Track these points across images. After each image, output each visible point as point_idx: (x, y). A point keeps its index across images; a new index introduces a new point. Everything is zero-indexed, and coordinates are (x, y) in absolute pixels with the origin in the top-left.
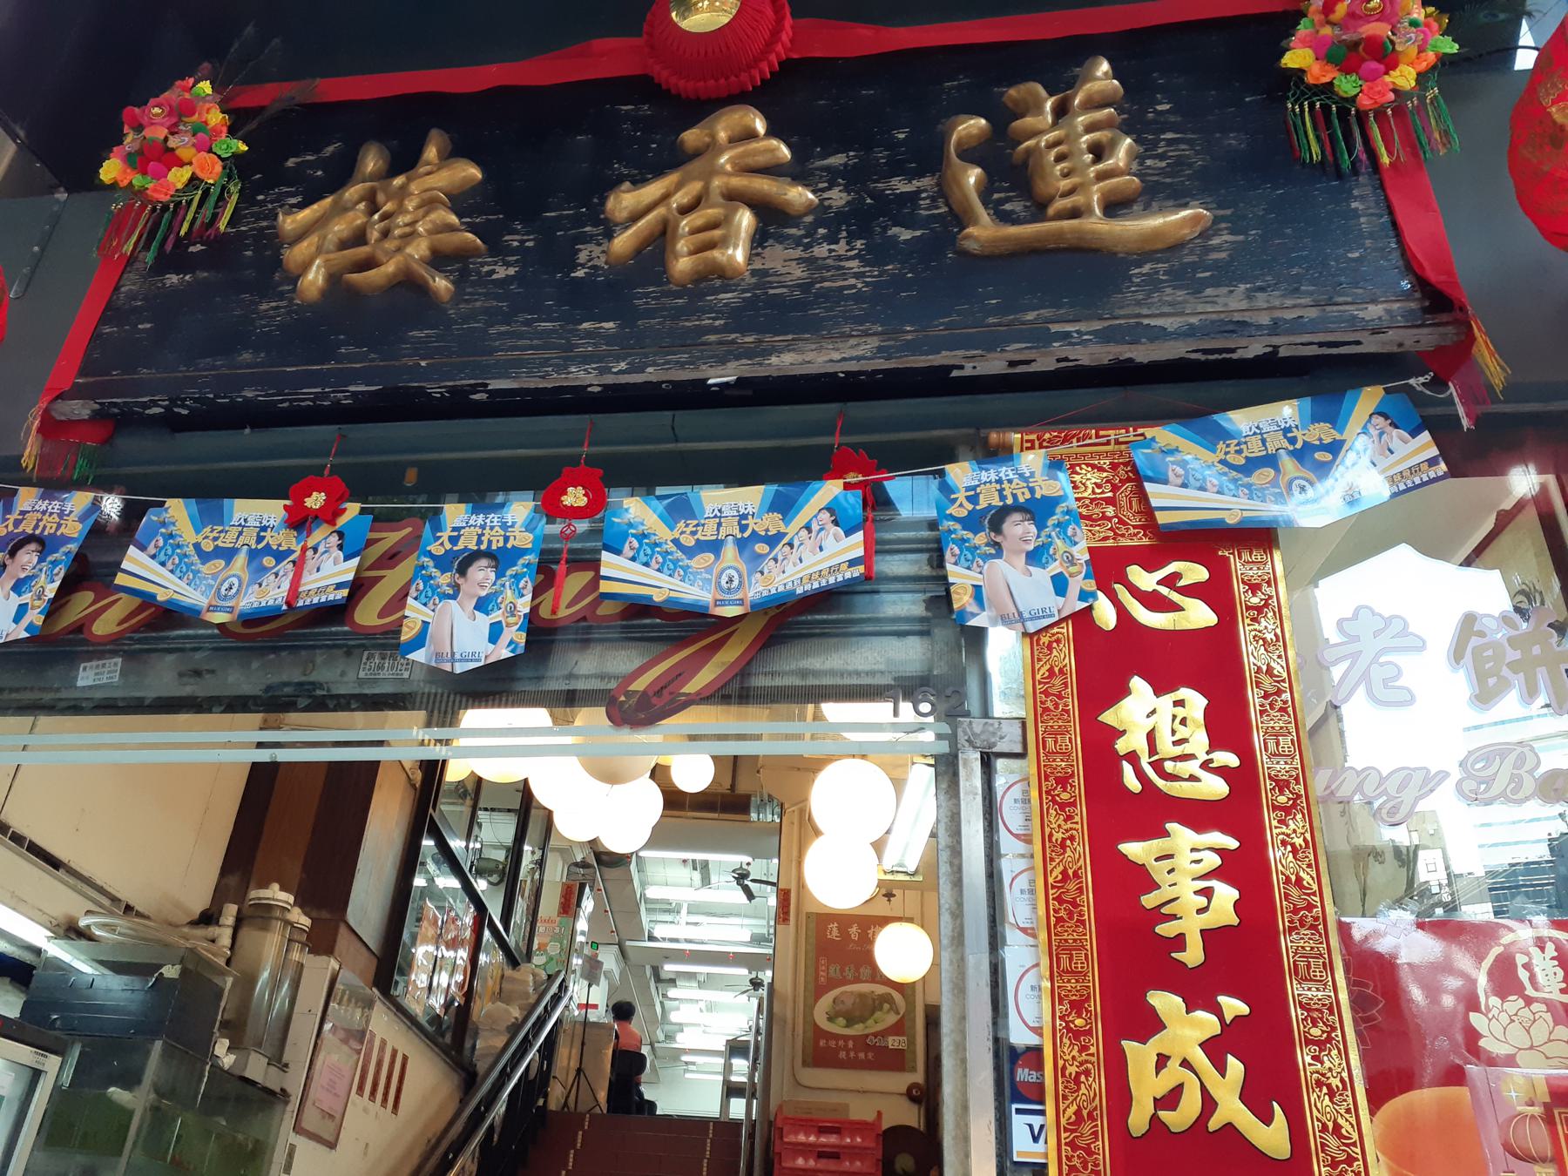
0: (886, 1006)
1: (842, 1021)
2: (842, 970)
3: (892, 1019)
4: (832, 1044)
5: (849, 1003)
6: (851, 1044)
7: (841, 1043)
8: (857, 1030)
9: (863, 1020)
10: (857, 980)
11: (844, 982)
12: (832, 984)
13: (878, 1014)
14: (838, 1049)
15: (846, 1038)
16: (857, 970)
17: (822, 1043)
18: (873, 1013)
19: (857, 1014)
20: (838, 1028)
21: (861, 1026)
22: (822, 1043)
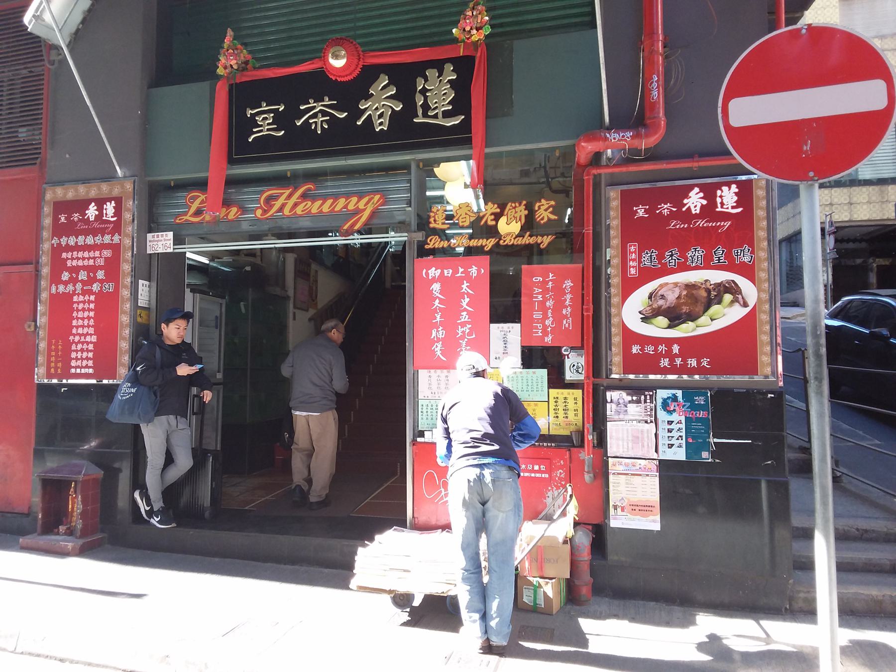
0: (728, 297)
1: (662, 321)
2: (660, 257)
3: (736, 313)
4: (650, 349)
5: (672, 297)
6: (676, 349)
7: (662, 348)
8: (686, 330)
9: (692, 317)
10: (684, 267)
11: (665, 271)
12: (647, 275)
13: (715, 309)
14: (658, 356)
15: (669, 342)
16: (683, 255)
17: (635, 349)
18: (707, 307)
19: (685, 309)
20: (658, 329)
21: (690, 325)
22: (635, 349)
